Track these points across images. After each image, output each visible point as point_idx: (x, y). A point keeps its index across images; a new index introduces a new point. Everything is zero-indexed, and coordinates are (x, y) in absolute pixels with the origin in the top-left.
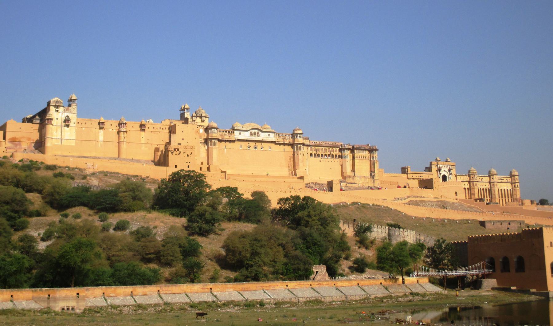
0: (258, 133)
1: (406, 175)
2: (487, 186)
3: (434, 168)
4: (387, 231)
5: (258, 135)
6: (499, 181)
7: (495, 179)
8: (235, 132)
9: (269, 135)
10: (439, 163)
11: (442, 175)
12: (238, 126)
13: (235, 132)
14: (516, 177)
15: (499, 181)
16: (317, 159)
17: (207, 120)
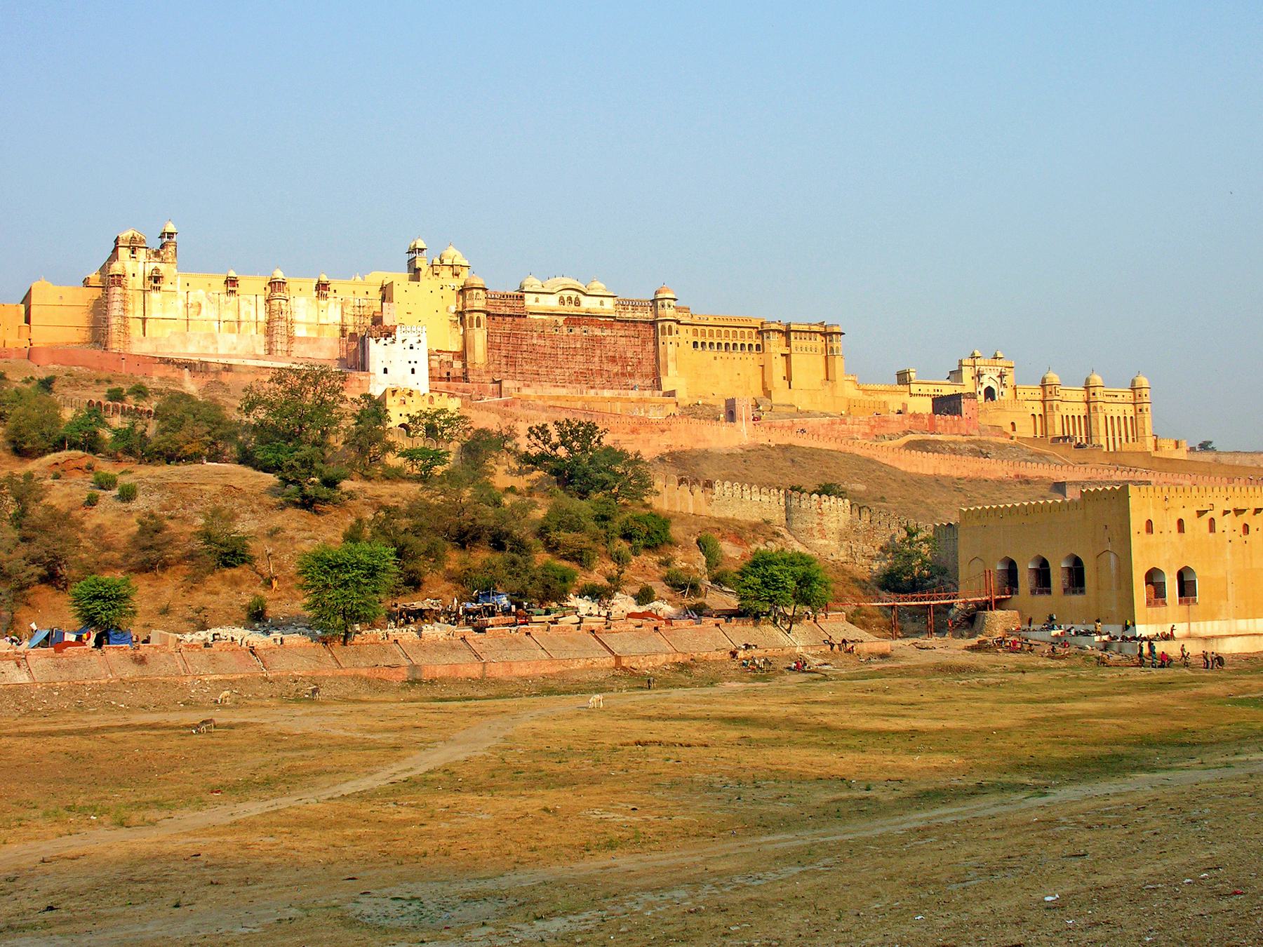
0: (577, 299)
1: (905, 388)
2: (1081, 410)
3: (967, 374)
4: (783, 500)
5: (578, 303)
6: (1108, 399)
7: (1098, 395)
8: (527, 296)
9: (602, 303)
10: (978, 361)
11: (985, 386)
12: (533, 283)
13: (527, 296)
14: (1144, 391)
15: (1108, 399)
16: (709, 354)
17: (465, 274)
